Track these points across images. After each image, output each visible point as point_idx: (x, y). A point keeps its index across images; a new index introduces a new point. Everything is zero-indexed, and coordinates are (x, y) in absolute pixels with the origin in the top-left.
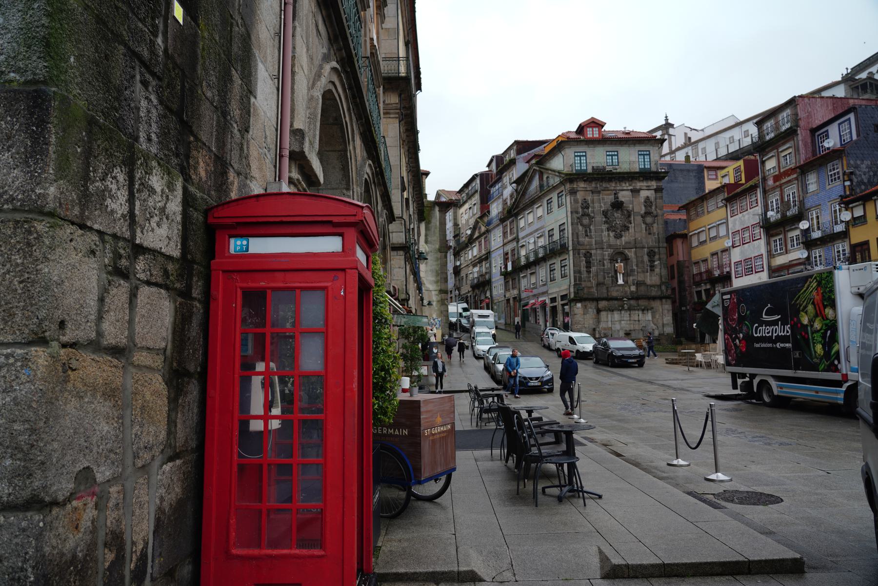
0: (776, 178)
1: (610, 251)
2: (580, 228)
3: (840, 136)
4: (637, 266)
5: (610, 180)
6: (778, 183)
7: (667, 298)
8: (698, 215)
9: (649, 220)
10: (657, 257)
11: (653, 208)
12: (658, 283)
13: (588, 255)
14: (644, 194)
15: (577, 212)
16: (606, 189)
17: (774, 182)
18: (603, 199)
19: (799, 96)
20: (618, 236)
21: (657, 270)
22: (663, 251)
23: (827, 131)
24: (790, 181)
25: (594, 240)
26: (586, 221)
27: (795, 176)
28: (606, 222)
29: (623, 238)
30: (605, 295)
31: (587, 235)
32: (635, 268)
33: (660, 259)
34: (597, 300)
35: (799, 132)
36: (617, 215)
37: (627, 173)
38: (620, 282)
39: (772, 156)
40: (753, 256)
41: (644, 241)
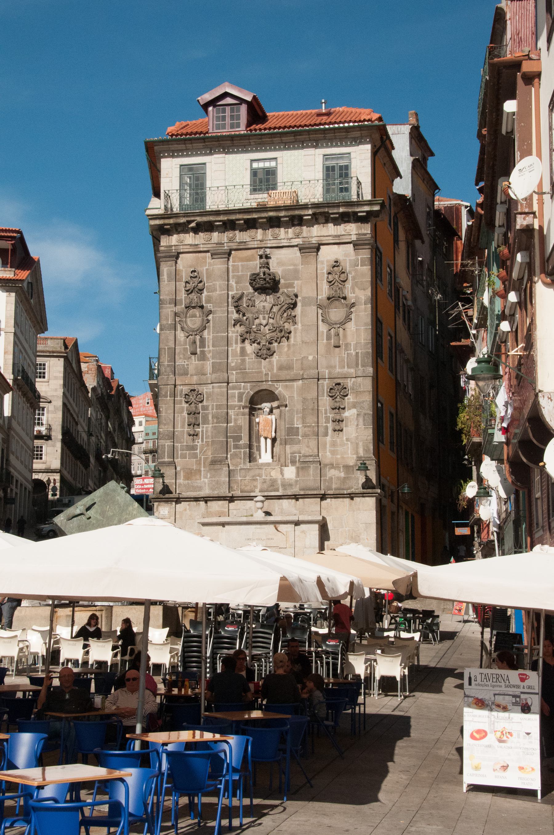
1: (248, 390)
2: (181, 335)
4: (304, 419)
5: (251, 225)
7: (363, 495)
9: (336, 313)
10: (350, 398)
11: (349, 285)
12: (351, 462)
13: (194, 397)
14: (328, 254)
15: (176, 303)
16: (243, 247)
18: (236, 269)
20: (265, 353)
22: (367, 385)
25: (208, 366)
26: (194, 320)
28: (237, 322)
29: (275, 358)
30: (224, 491)
31: (194, 353)
32: (298, 424)
33: (354, 406)
34: (206, 500)
36: (264, 302)
37: (287, 208)
38: (265, 457)
41: (323, 362)
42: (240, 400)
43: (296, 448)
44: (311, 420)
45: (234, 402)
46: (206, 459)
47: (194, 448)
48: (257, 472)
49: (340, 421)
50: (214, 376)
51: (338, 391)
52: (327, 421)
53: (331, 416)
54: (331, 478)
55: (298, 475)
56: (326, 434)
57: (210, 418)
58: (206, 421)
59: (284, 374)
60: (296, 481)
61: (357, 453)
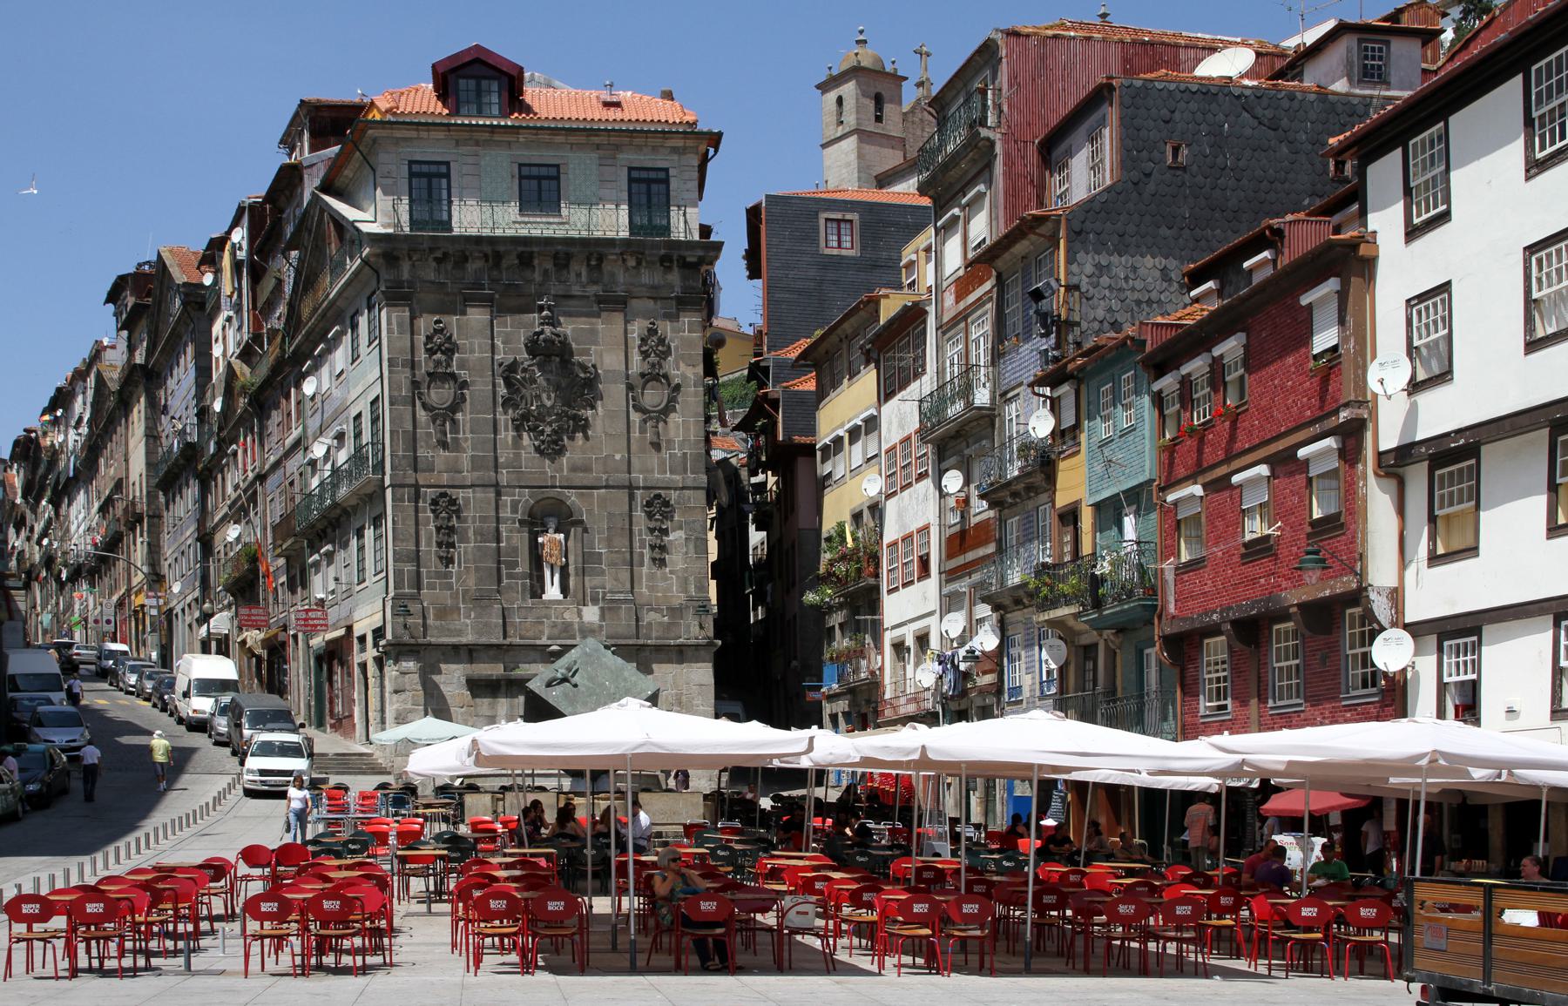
0: (963, 286)
4: (609, 542)
8: (835, 384)
12: (676, 603)
17: (958, 299)
19: (1013, 34)
21: (676, 560)
24: (979, 303)
27: (987, 286)
35: (998, 149)
38: (553, 592)
40: (913, 527)
42: (515, 510)
43: (597, 581)
44: (621, 543)
45: (506, 513)
46: (465, 592)
47: (448, 575)
48: (544, 612)
49: (663, 548)
50: (476, 474)
51: (659, 507)
52: (642, 546)
53: (648, 538)
54: (650, 624)
55: (602, 617)
56: (642, 564)
57: (471, 533)
58: (464, 539)
59: (580, 478)
60: (601, 627)
61: (686, 591)
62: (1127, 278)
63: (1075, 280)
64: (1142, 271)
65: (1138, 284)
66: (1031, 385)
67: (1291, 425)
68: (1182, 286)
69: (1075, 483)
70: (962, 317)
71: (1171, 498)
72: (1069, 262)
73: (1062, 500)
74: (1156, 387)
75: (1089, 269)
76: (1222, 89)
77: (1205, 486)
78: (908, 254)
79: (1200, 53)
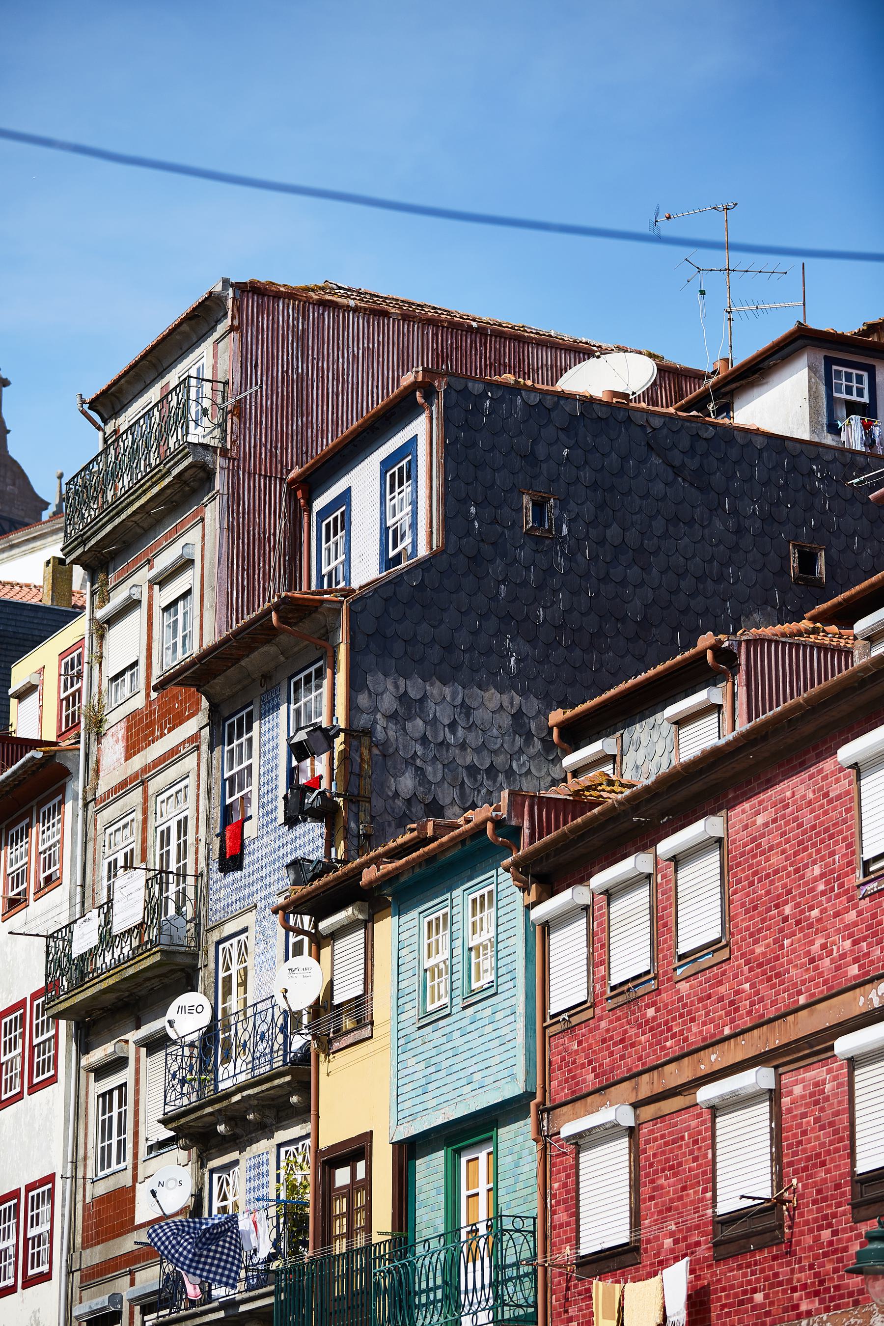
3: (384, 530)
6: (138, 762)
17: (132, 749)
23: (345, 497)
24: (172, 756)
27: (190, 727)
35: (219, 483)
39: (131, 605)
62: (453, 726)
63: (363, 721)
64: (479, 715)
65: (475, 739)
66: (283, 910)
67: (821, 990)
68: (548, 745)
69: (358, 1096)
70: (140, 780)
71: (568, 1129)
72: (354, 685)
73: (334, 1131)
74: (539, 913)
75: (388, 703)
76: (613, 412)
77: (636, 1106)
78: (21, 674)
79: (563, 358)
